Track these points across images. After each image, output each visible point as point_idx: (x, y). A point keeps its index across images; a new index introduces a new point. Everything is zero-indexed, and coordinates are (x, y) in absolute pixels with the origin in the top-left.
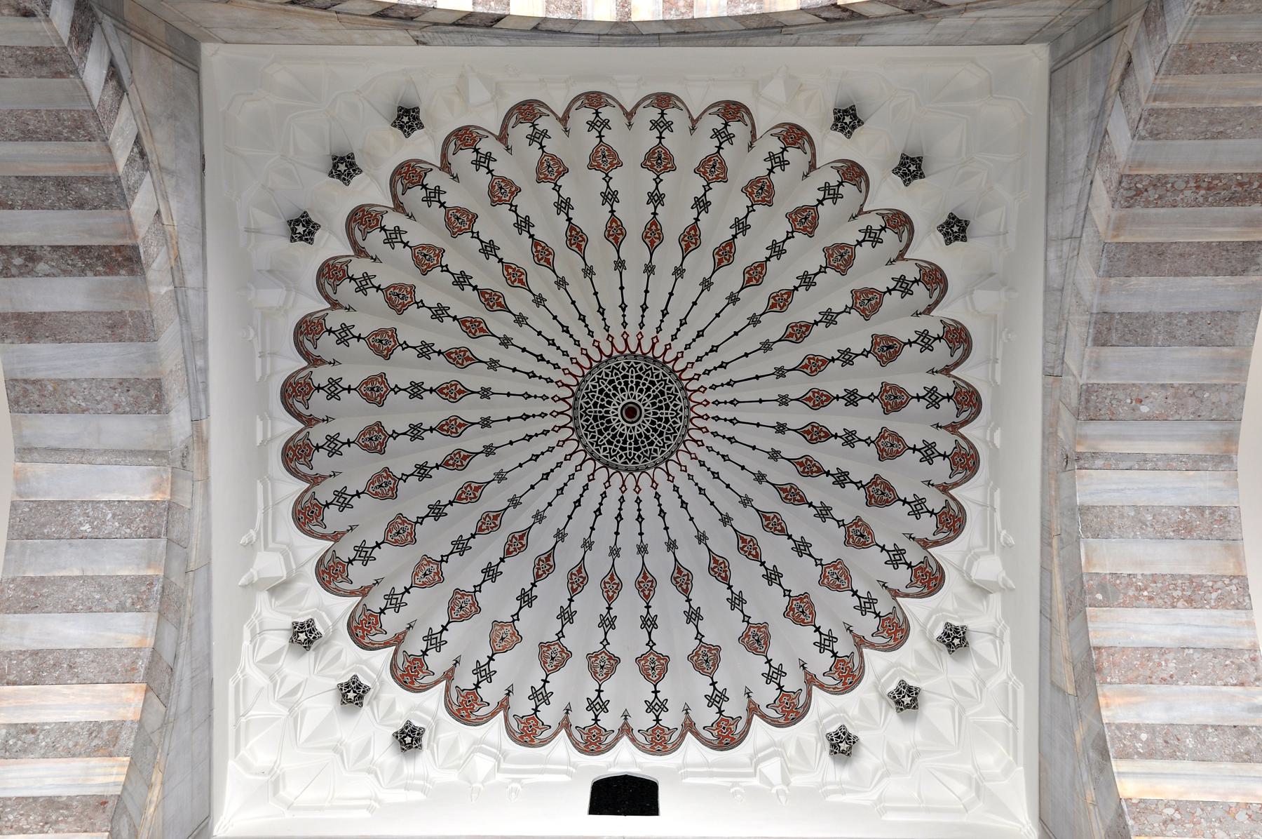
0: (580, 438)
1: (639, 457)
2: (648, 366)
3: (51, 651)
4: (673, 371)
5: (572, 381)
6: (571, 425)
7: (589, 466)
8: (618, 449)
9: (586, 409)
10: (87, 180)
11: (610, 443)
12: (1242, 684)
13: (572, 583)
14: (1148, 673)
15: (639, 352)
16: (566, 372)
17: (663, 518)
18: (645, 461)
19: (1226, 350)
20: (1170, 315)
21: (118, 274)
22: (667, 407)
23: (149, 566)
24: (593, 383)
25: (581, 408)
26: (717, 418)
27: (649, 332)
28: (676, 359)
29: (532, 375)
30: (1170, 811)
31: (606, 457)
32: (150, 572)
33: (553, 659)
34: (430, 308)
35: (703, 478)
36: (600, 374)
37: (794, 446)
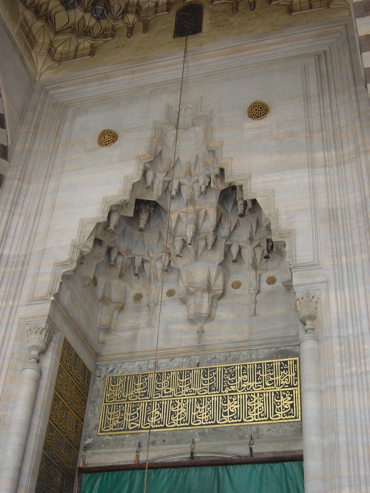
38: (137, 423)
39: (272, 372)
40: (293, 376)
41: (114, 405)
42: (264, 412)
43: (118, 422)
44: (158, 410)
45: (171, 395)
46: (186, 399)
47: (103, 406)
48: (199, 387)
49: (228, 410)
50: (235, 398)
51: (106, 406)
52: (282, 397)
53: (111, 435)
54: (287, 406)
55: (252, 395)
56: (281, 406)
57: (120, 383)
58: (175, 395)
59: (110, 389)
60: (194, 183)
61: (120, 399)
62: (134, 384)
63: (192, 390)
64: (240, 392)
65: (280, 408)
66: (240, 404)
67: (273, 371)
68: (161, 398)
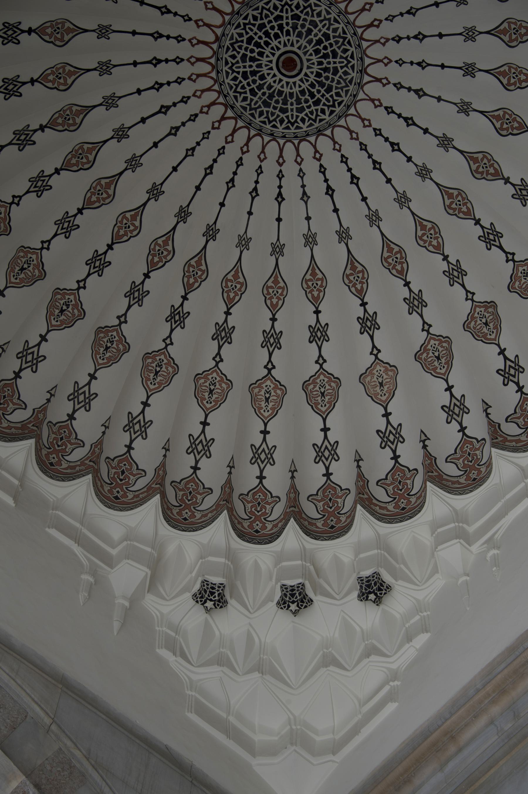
0: (272, 135)
1: (338, 94)
2: (257, 9)
5: (212, 96)
6: (253, 132)
7: (306, 149)
8: (313, 108)
9: (250, 105)
11: (300, 110)
13: (394, 268)
16: (198, 93)
17: (414, 124)
18: (347, 91)
24: (231, 77)
25: (245, 109)
29: (174, 131)
31: (311, 125)
33: (438, 358)
34: (28, 192)
36: (227, 63)
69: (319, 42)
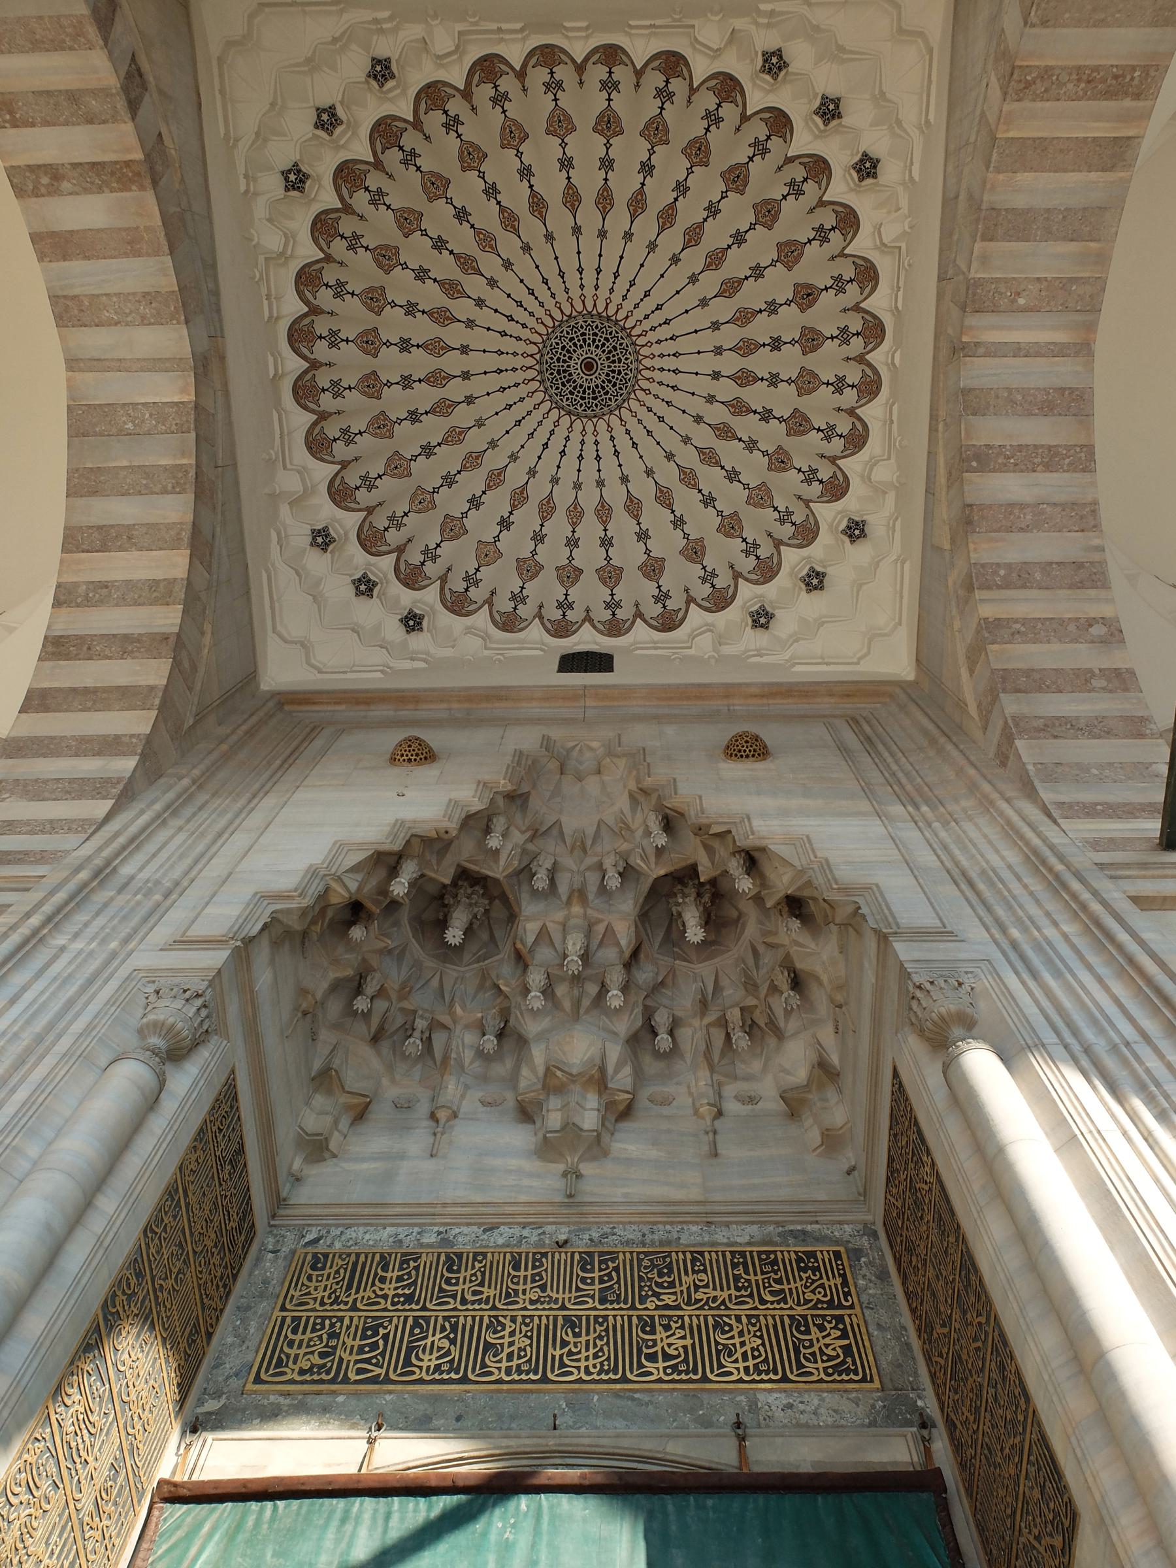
3: (112, 526)
4: (624, 329)
10: (94, 93)
11: (571, 393)
12: (1083, 531)
14: (1009, 524)
15: (595, 312)
19: (1093, 245)
20: (1048, 210)
21: (130, 190)
22: (620, 361)
23: (183, 454)
26: (662, 369)
27: (603, 293)
28: (627, 317)
29: (503, 334)
30: (1017, 626)
32: (185, 461)
35: (650, 421)
37: (727, 390)
38: (376, 1365)
39: (776, 1273)
40: (836, 1285)
41: (308, 1318)
42: (766, 1360)
43: (317, 1360)
44: (447, 1337)
45: (487, 1302)
46: (531, 1317)
47: (274, 1318)
48: (570, 1292)
49: (658, 1348)
50: (676, 1322)
51: (284, 1318)
52: (813, 1329)
53: (287, 1394)
54: (834, 1349)
55: (725, 1319)
56: (816, 1348)
57: (335, 1268)
58: (499, 1306)
59: (303, 1279)
60: (587, 869)
61: (332, 1304)
62: (376, 1274)
63: (548, 1296)
64: (688, 1311)
65: (813, 1354)
66: (692, 1337)
67: (779, 1269)
68: (455, 1309)
69: (614, 372)
